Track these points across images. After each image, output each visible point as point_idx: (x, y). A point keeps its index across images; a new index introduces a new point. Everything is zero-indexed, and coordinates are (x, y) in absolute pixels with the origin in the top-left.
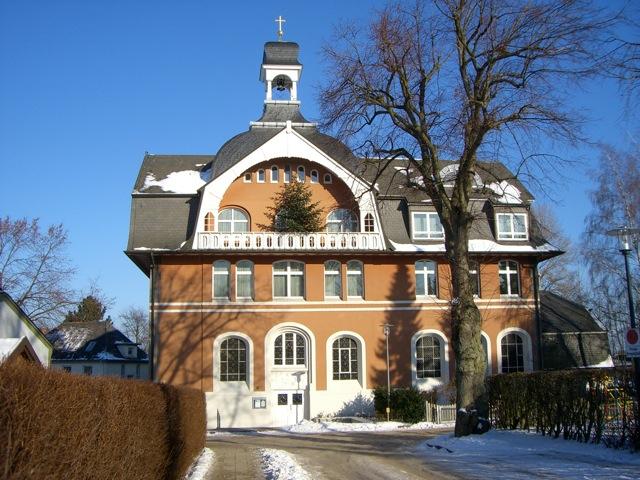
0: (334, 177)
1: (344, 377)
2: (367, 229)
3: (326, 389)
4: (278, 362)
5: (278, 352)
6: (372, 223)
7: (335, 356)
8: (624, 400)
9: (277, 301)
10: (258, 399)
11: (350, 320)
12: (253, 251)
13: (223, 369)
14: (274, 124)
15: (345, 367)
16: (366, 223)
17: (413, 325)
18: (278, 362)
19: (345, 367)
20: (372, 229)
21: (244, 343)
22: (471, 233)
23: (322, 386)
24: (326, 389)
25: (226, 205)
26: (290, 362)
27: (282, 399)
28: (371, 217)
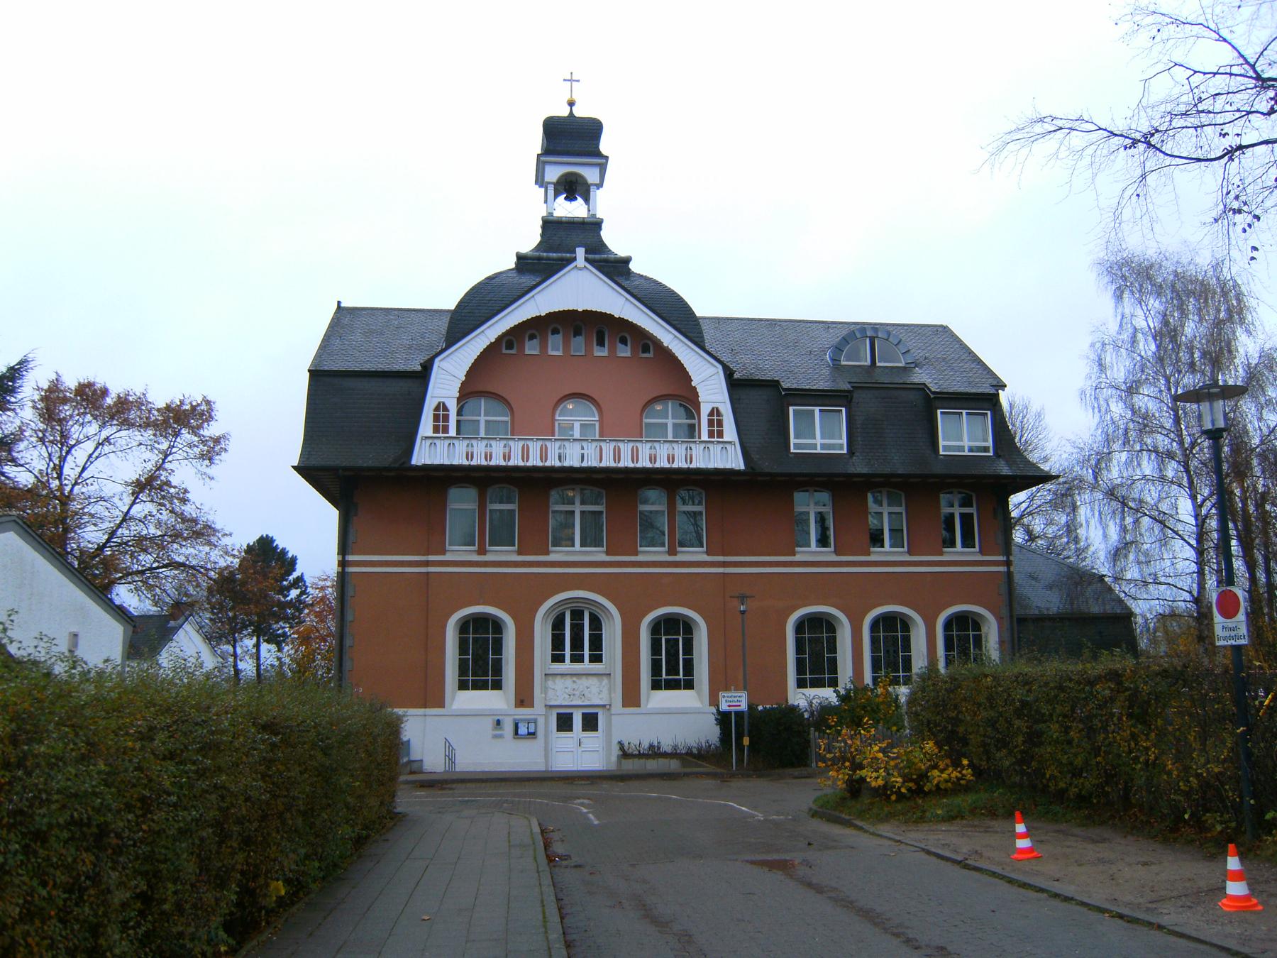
0: (658, 344)
1: (673, 685)
2: (711, 434)
3: (533, 707)
4: (558, 658)
5: (557, 643)
6: (720, 423)
7: (655, 648)
8: (843, 784)
9: (557, 555)
10: (523, 720)
11: (683, 587)
12: (516, 469)
13: (463, 669)
14: (568, 255)
15: (672, 669)
16: (711, 423)
17: (279, 554)
18: (558, 658)
19: (672, 669)
20: (720, 434)
21: (498, 626)
22: (618, 350)
23: (631, 698)
24: (533, 707)
25: (469, 392)
26: (577, 658)
27: (564, 723)
28: (719, 414)
